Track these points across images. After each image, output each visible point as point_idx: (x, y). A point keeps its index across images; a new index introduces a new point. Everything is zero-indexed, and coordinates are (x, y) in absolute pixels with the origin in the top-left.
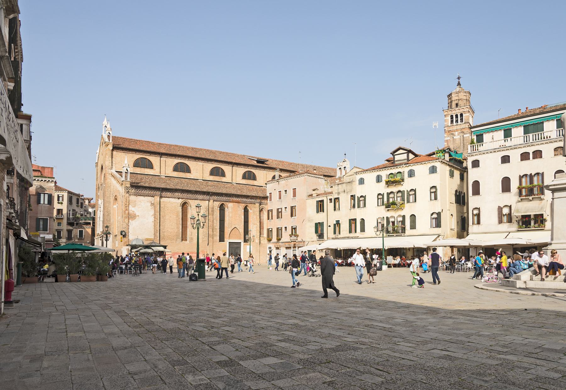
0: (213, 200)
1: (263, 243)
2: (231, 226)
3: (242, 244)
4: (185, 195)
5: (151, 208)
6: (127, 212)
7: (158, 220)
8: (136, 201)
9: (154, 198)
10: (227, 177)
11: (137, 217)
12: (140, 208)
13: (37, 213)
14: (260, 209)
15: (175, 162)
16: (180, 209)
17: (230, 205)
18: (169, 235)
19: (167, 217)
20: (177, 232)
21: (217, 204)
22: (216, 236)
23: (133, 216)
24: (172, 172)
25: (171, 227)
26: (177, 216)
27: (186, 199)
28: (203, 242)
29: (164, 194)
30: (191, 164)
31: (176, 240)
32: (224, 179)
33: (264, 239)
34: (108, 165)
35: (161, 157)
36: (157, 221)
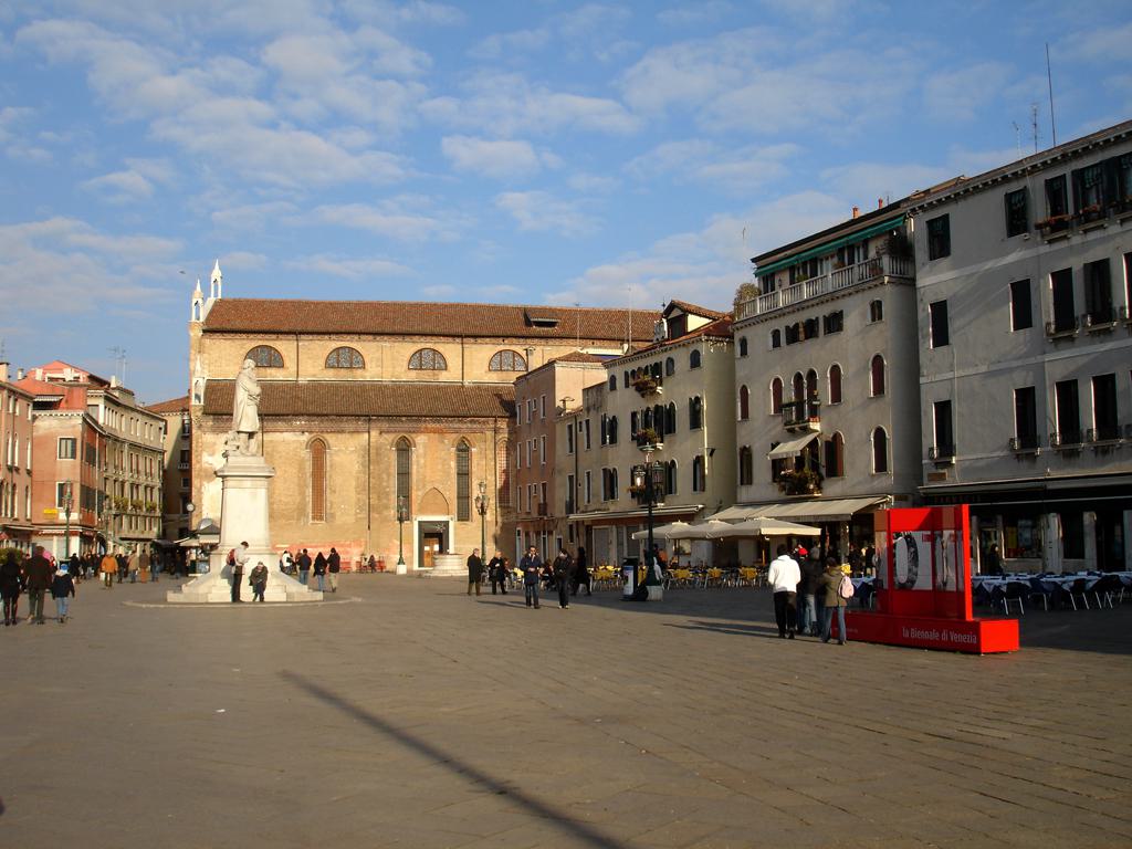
2: (424, 486)
4: (316, 423)
6: (198, 466)
8: (215, 444)
13: (54, 475)
16: (306, 455)
17: (421, 441)
21: (390, 438)
22: (387, 507)
26: (301, 469)
30: (366, 347)
31: (298, 519)
32: (444, 377)
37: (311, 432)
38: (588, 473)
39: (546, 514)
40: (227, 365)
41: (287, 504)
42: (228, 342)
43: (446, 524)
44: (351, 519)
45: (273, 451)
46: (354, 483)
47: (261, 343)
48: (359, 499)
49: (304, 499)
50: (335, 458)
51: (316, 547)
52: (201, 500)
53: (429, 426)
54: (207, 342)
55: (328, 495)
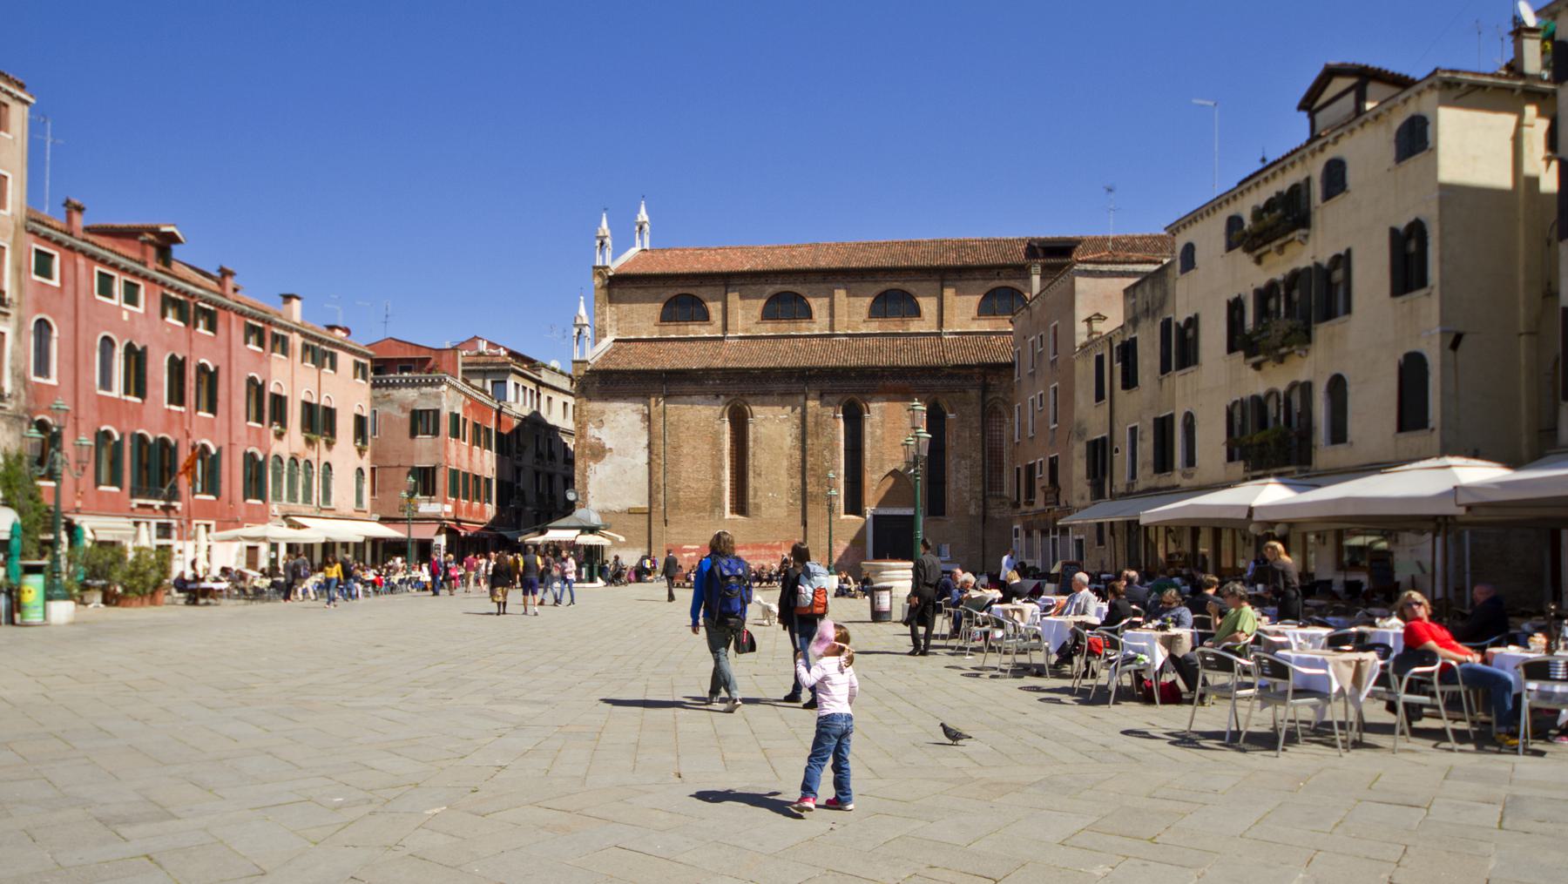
0: (819, 392)
1: (997, 516)
2: (881, 467)
3: (920, 520)
7: (660, 458)
8: (603, 412)
10: (927, 318)
11: (608, 454)
12: (614, 428)
13: (412, 457)
14: (984, 407)
18: (691, 499)
20: (712, 490)
23: (596, 452)
28: (789, 515)
31: (712, 511)
33: (1003, 503)
35: (727, 286)
37: (727, 395)
38: (1133, 430)
39: (1058, 503)
40: (639, 321)
41: (698, 489)
43: (911, 520)
44: (782, 513)
45: (679, 420)
46: (785, 463)
47: (680, 291)
48: (792, 484)
49: (719, 485)
50: (762, 430)
52: (585, 486)
53: (888, 383)
54: (616, 291)
55: (752, 481)
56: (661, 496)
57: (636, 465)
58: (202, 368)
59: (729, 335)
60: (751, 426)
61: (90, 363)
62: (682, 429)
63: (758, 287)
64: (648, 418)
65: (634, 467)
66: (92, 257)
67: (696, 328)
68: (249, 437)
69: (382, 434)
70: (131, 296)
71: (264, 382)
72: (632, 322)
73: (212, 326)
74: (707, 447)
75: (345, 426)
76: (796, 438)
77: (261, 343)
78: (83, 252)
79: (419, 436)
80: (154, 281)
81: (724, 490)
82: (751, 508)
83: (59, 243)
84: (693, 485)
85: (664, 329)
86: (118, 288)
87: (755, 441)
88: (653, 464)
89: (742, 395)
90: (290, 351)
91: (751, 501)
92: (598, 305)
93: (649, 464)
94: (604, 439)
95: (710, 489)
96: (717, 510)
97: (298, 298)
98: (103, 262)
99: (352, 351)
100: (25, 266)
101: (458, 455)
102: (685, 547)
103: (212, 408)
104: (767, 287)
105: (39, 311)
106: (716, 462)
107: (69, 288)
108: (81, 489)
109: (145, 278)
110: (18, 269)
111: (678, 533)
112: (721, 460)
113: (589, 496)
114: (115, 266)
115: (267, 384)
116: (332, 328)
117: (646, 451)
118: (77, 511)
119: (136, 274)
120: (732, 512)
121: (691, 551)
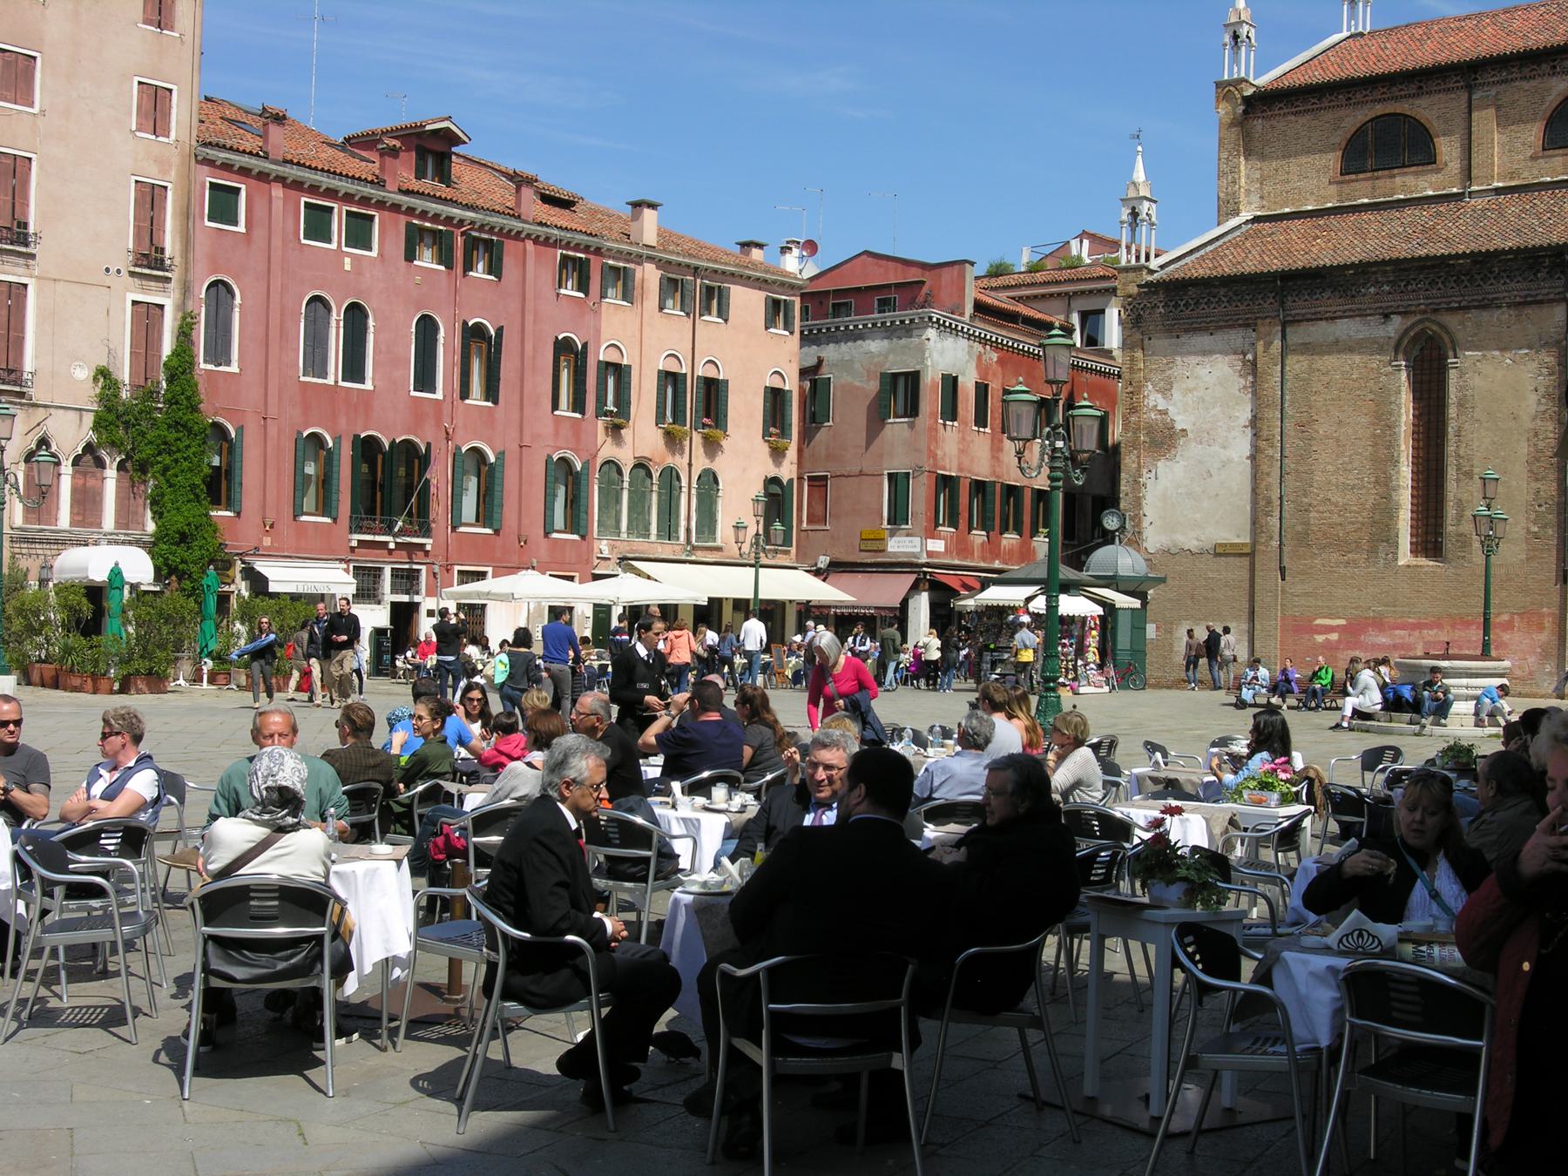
5: (1245, 387)
9: (1254, 334)
12: (1190, 391)
15: (1554, 93)
18: (1331, 526)
19: (1322, 429)
24: (1533, 158)
25: (1341, 479)
27: (1425, 312)
28: (1528, 559)
29: (1298, 306)
31: (1373, 551)
34: (1227, 194)
35: (1470, 88)
36: (1270, 452)
37: (1404, 314)
42: (1303, 120)
46: (1524, 449)
47: (1379, 109)
50: (1476, 381)
51: (1418, 626)
52: (1138, 503)
54: (1258, 125)
56: (1274, 521)
57: (1230, 461)
58: (473, 334)
59: (1474, 188)
60: (1453, 374)
61: (286, 336)
62: (1317, 386)
63: (1533, 83)
64: (1253, 368)
65: (1225, 464)
66: (298, 185)
67: (1410, 180)
68: (557, 434)
69: (837, 419)
70: (359, 234)
71: (585, 345)
72: (1288, 182)
73: (495, 268)
74: (1364, 420)
75: (745, 410)
76: (1548, 395)
77: (583, 286)
78: (281, 179)
79: (891, 420)
80: (395, 208)
81: (1398, 507)
82: (1449, 545)
83: (244, 172)
84: (1336, 498)
85: (1346, 189)
86: (338, 224)
87: (1460, 405)
88: (1260, 456)
89: (1435, 311)
90: (637, 293)
91: (1450, 528)
92: (1224, 155)
93: (1253, 458)
94: (1173, 411)
95: (1371, 501)
96: (1382, 547)
97: (652, 206)
98: (313, 190)
99: (760, 284)
100: (195, 209)
101: (962, 451)
102: (1319, 621)
103: (491, 392)
104: (1554, 81)
105: (214, 272)
106: (1383, 452)
107: (260, 233)
108: (269, 522)
109: (381, 205)
110: (186, 215)
111: (1307, 594)
112: (1391, 445)
113: (1145, 523)
114: (331, 193)
115: (591, 349)
116: (746, 245)
117: (1249, 431)
118: (257, 552)
119: (365, 201)
120: (1415, 551)
121: (1330, 629)
